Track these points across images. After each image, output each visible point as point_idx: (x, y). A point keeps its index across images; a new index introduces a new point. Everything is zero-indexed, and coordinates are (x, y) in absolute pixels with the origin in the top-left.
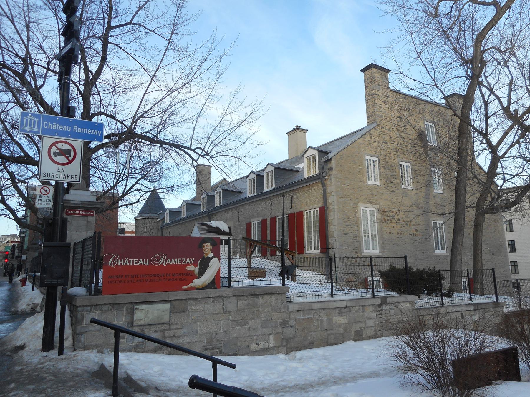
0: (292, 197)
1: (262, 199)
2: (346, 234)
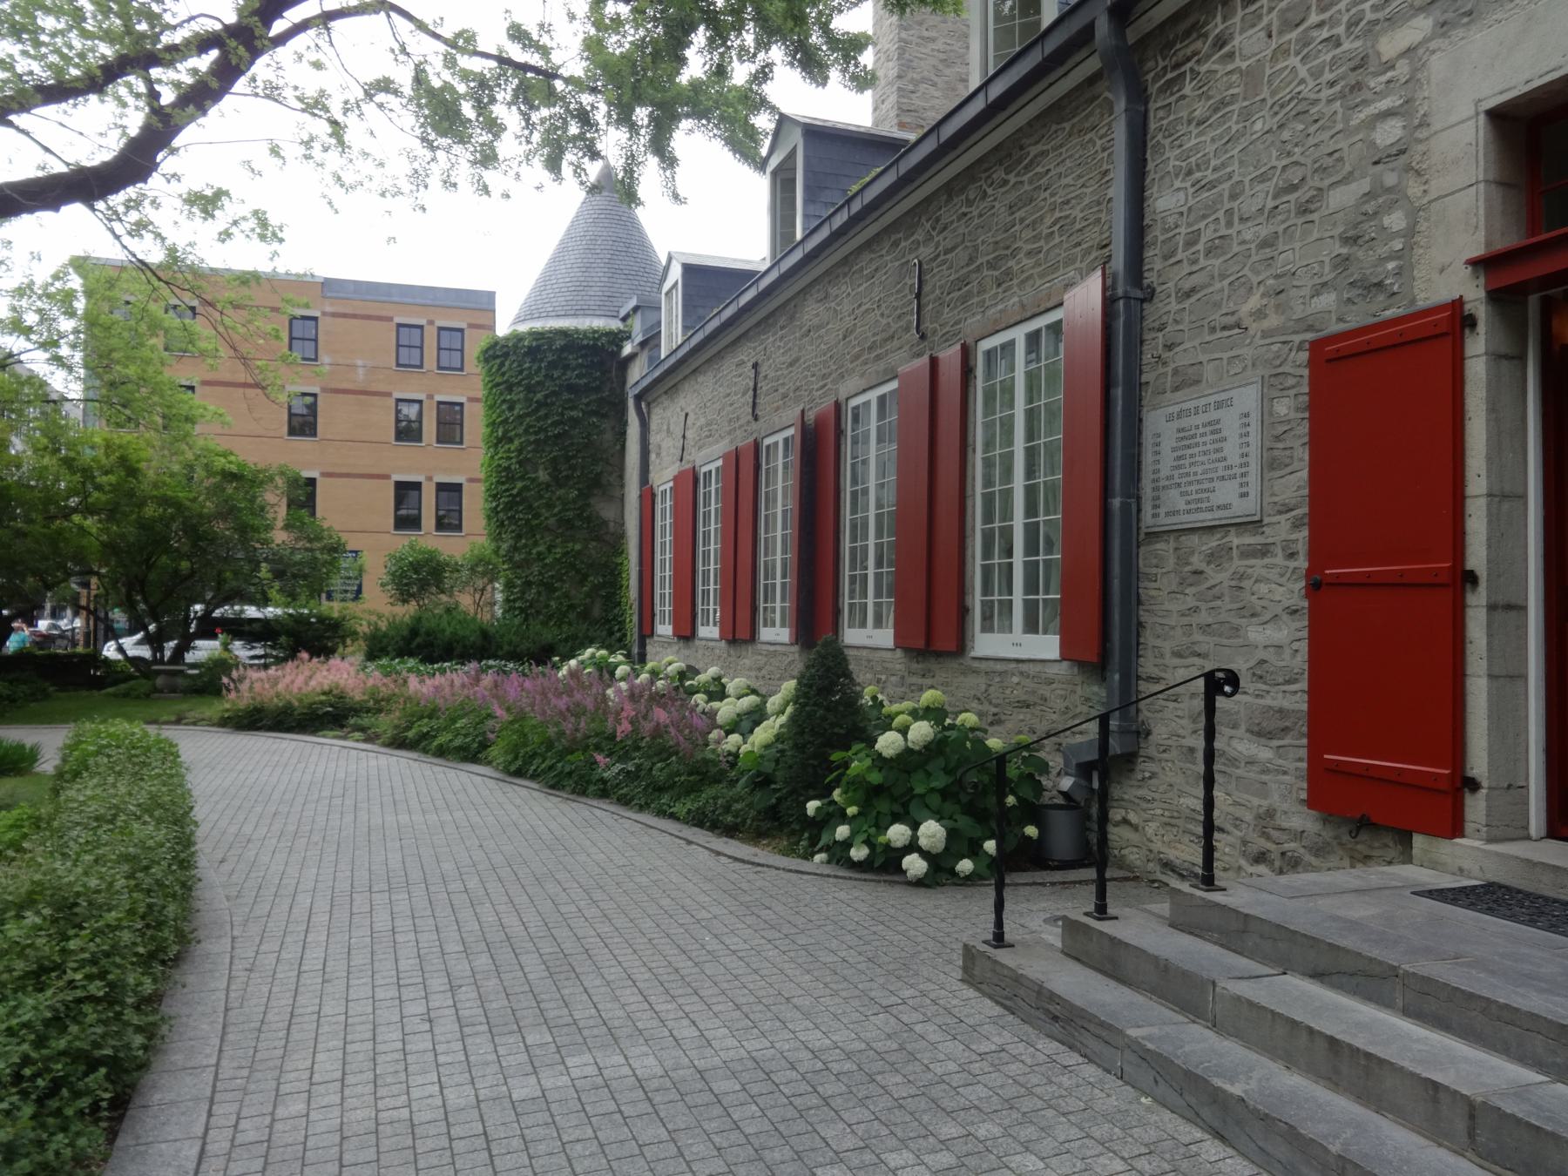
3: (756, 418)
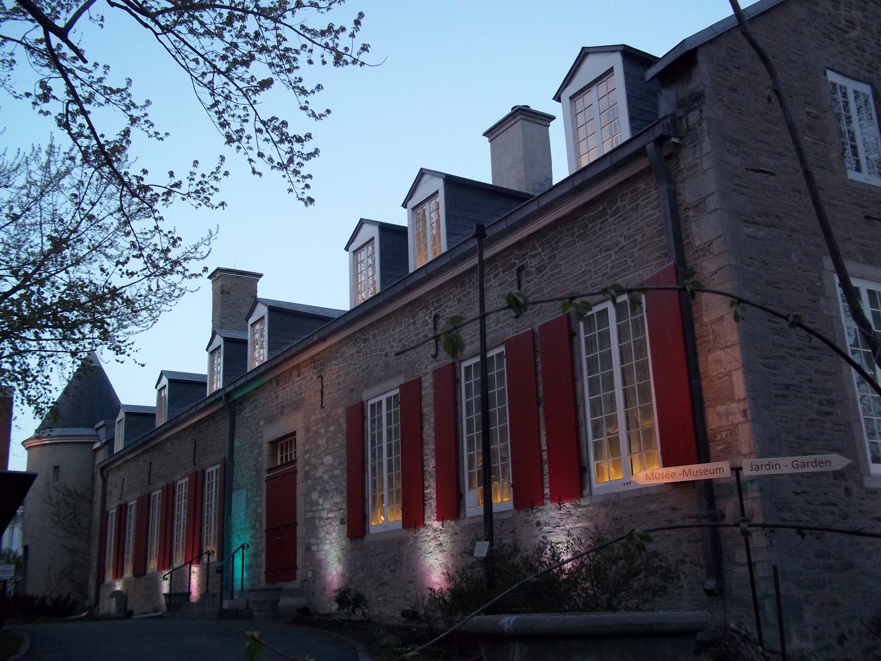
0: (520, 270)
1: (403, 308)
2: (788, 387)
3: (149, 484)
